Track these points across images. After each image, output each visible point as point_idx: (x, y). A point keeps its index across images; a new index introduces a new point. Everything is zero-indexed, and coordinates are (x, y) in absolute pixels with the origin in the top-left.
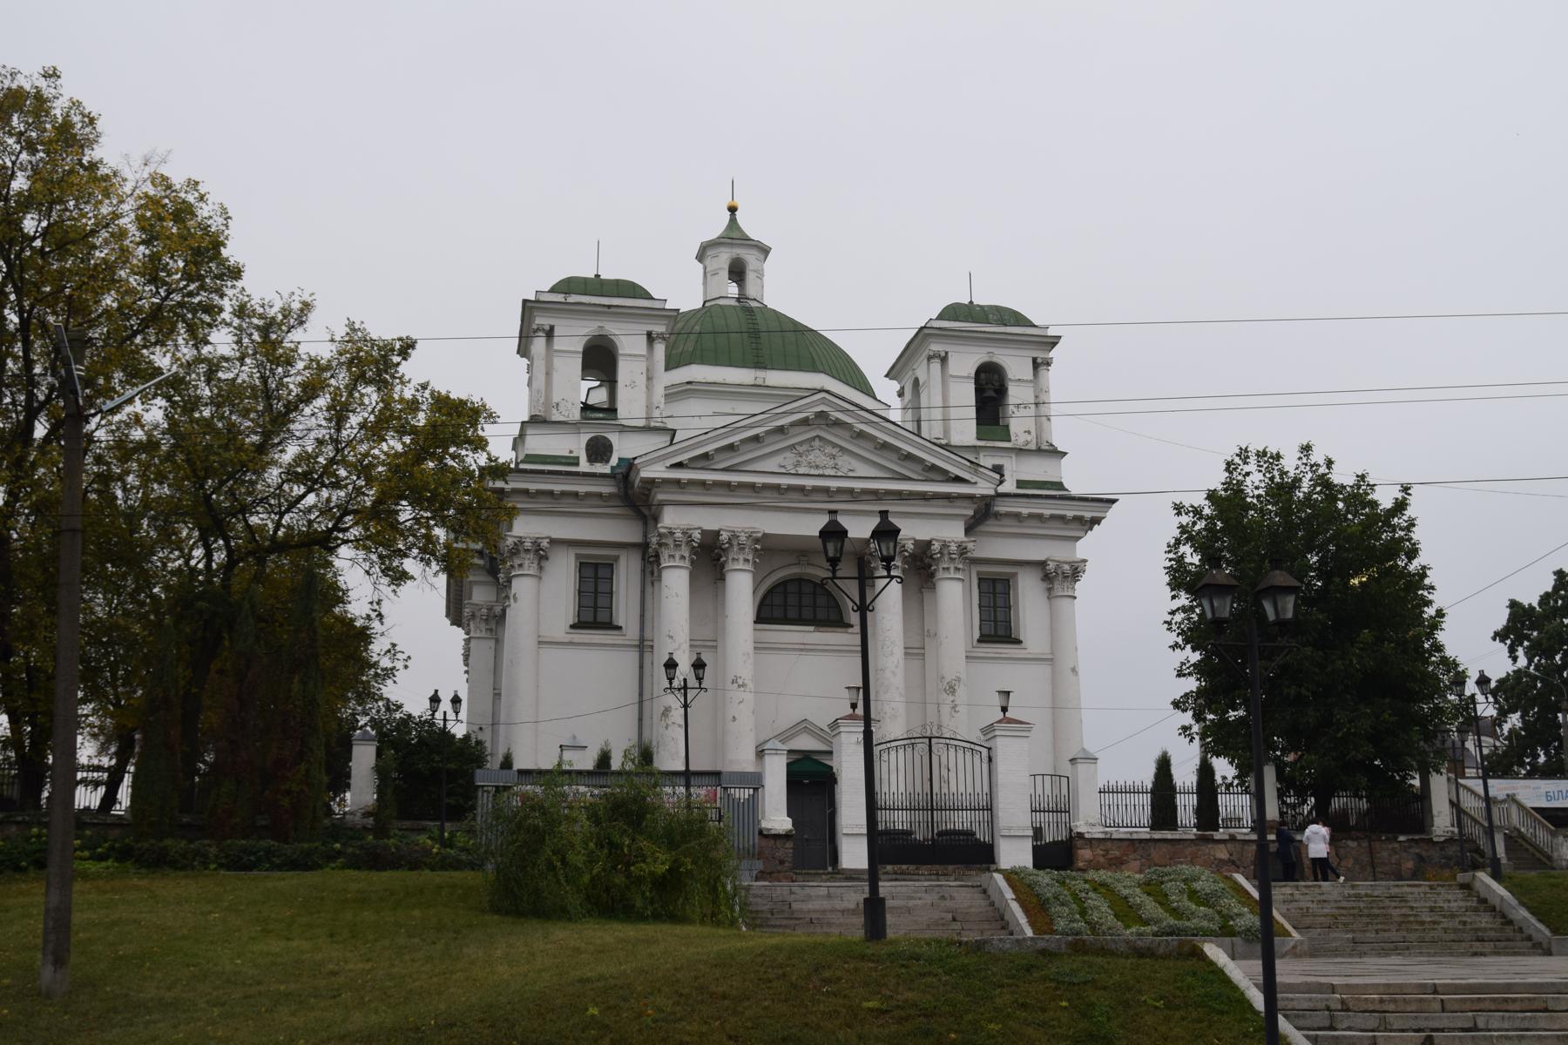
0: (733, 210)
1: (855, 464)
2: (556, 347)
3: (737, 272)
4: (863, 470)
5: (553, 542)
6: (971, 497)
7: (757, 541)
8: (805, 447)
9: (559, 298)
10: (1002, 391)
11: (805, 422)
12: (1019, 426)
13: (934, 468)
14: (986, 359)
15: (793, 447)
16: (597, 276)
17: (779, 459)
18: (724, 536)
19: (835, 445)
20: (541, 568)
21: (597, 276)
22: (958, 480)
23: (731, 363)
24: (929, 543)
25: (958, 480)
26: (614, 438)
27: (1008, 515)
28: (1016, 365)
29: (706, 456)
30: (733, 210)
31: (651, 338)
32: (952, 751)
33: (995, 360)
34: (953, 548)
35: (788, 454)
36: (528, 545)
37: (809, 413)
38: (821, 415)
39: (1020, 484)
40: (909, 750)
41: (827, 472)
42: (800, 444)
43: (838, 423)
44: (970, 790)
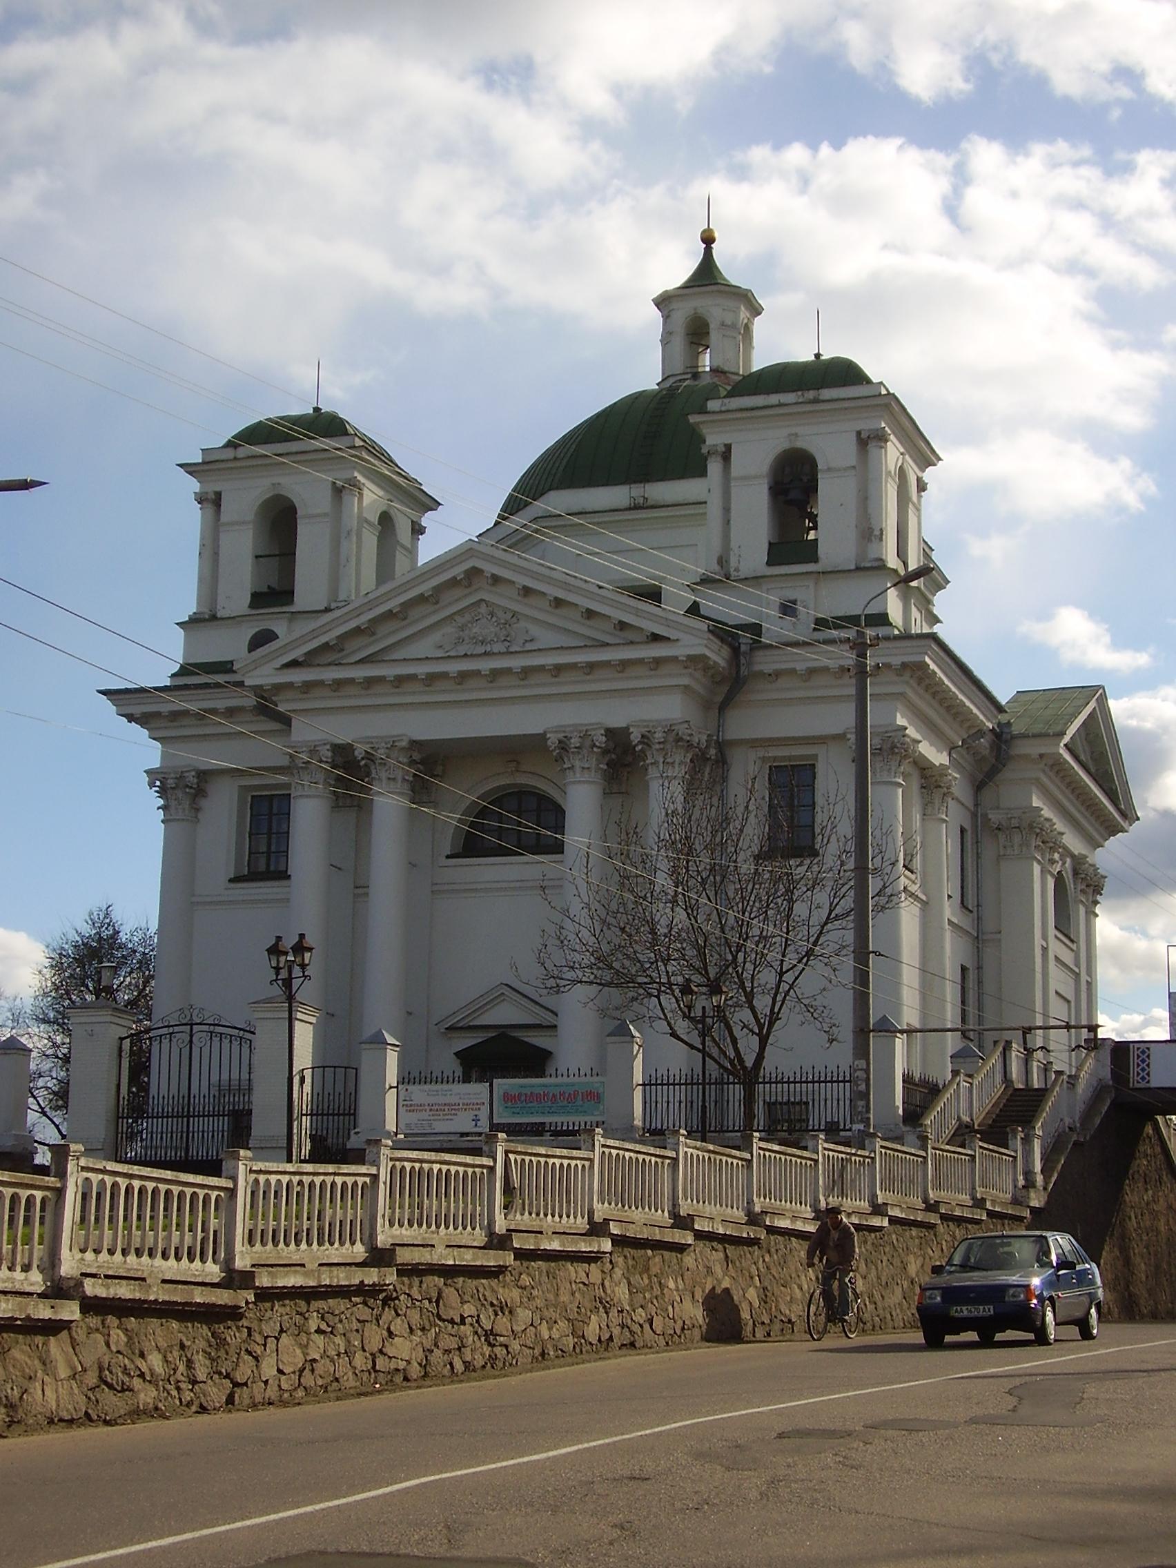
0: (708, 239)
1: (535, 630)
2: (224, 518)
3: (698, 334)
4: (547, 638)
5: (205, 776)
6: (674, 659)
7: (403, 749)
8: (468, 617)
9: (230, 453)
10: (811, 488)
11: (453, 583)
12: (832, 534)
13: (622, 626)
14: (785, 445)
15: (450, 617)
16: (317, 410)
17: (436, 637)
18: (359, 754)
19: (506, 610)
20: (197, 810)
21: (317, 410)
22: (656, 638)
23: (607, 483)
24: (625, 731)
25: (656, 638)
26: (280, 628)
27: (777, 674)
28: (829, 444)
29: (326, 647)
30: (708, 239)
31: (338, 491)
32: (216, 1040)
33: (799, 444)
34: (659, 736)
35: (449, 629)
36: (575, 742)
37: (458, 571)
38: (474, 572)
39: (821, 623)
40: (166, 1042)
41: (497, 648)
42: (460, 612)
43: (496, 579)
44: (184, 1090)
